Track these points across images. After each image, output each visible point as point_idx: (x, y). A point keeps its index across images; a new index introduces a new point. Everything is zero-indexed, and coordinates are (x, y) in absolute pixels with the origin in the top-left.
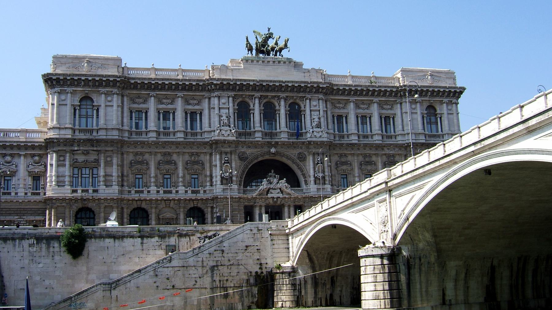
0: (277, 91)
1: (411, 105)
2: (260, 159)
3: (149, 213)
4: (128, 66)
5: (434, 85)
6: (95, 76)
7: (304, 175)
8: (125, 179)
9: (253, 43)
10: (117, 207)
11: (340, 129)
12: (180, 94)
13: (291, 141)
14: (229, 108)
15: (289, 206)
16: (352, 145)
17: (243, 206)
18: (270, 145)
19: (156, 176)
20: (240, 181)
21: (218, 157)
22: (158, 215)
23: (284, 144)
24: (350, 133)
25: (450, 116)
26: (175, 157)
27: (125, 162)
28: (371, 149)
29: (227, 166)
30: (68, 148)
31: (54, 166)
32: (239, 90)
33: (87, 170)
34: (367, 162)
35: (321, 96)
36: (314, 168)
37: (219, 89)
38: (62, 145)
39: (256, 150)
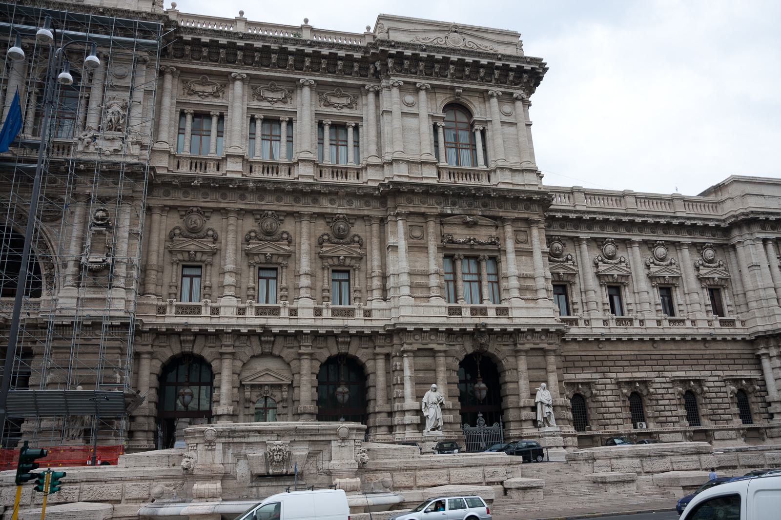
1: (401, 98)
34: (268, 233)
36: (83, 239)
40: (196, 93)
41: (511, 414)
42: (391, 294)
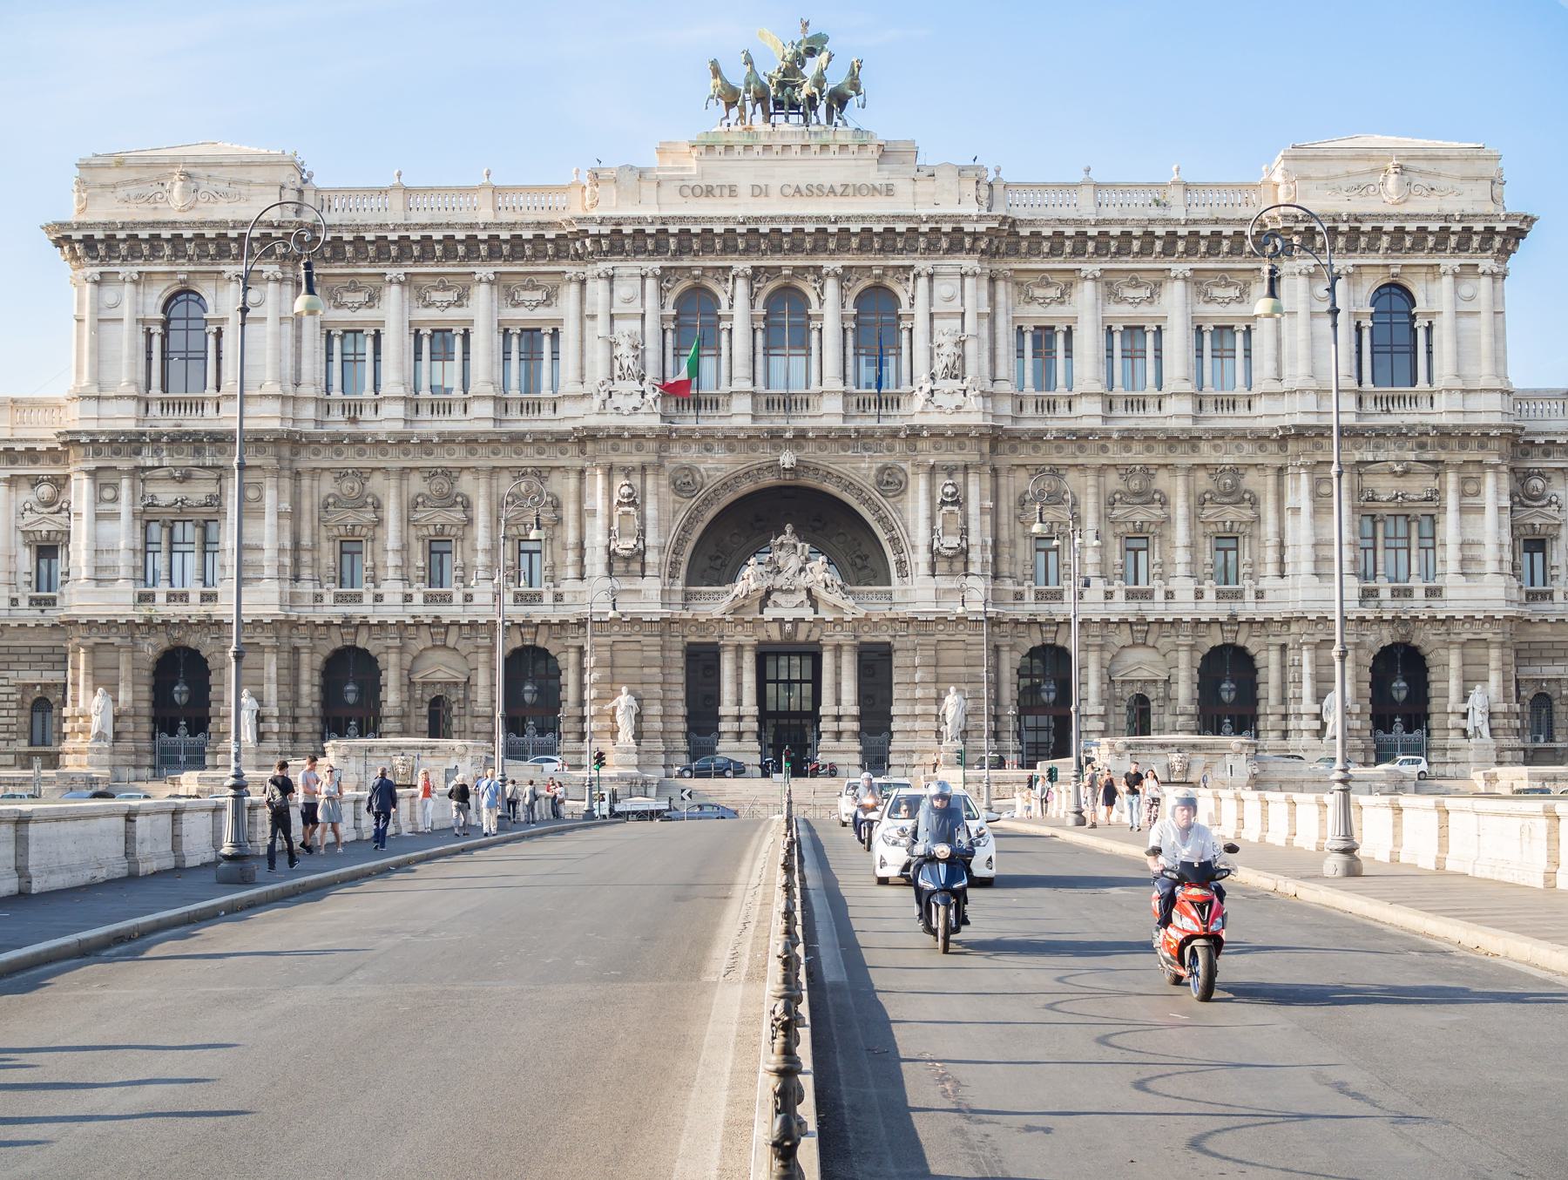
0: (814, 250)
1: (1311, 289)
2: (746, 487)
3: (381, 666)
4: (317, 182)
5: (1409, 209)
6: (203, 224)
7: (894, 541)
8: (306, 557)
9: (737, 76)
10: (277, 649)
11: (1045, 377)
12: (485, 271)
13: (852, 424)
14: (643, 316)
15: (838, 648)
16: (1081, 438)
17: (681, 646)
18: (775, 436)
19: (405, 548)
20: (674, 565)
21: (600, 481)
22: (410, 672)
23: (825, 437)
24: (1076, 390)
25: (1466, 322)
26: (466, 484)
27: (306, 504)
28: (1149, 449)
29: (627, 514)
30: (124, 464)
31: (84, 517)
32: (680, 252)
33: (189, 526)
34: (1138, 494)
35: (970, 263)
37: (612, 251)
38: (106, 450)
39: (729, 457)
40: (1033, 299)
41: (1434, 721)
42: (1289, 570)
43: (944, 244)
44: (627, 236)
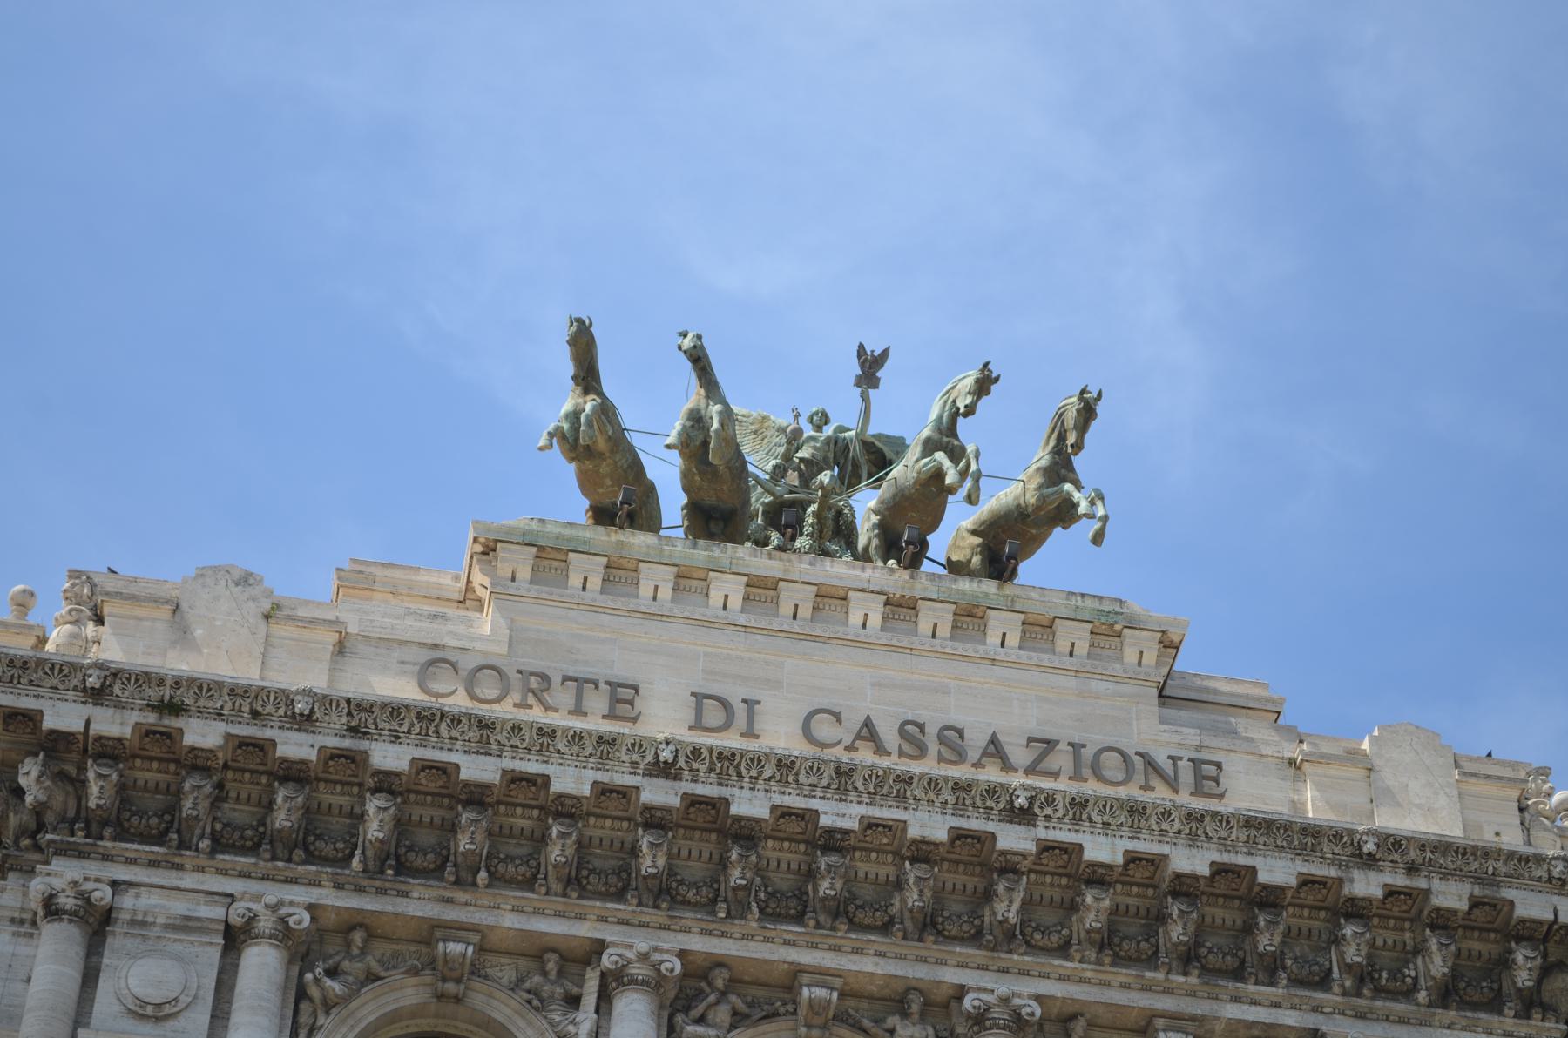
0: (929, 925)
37: (117, 824)
43: (1437, 964)
44: (198, 761)
